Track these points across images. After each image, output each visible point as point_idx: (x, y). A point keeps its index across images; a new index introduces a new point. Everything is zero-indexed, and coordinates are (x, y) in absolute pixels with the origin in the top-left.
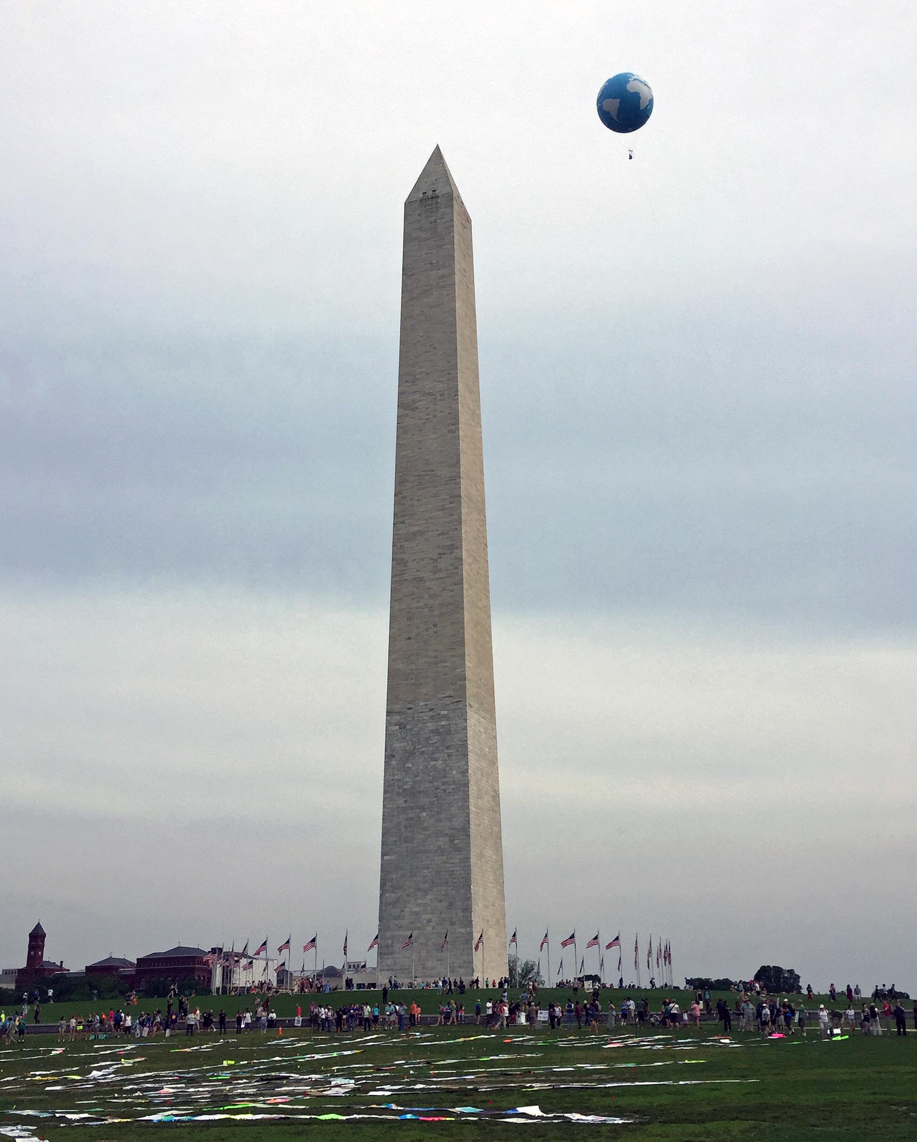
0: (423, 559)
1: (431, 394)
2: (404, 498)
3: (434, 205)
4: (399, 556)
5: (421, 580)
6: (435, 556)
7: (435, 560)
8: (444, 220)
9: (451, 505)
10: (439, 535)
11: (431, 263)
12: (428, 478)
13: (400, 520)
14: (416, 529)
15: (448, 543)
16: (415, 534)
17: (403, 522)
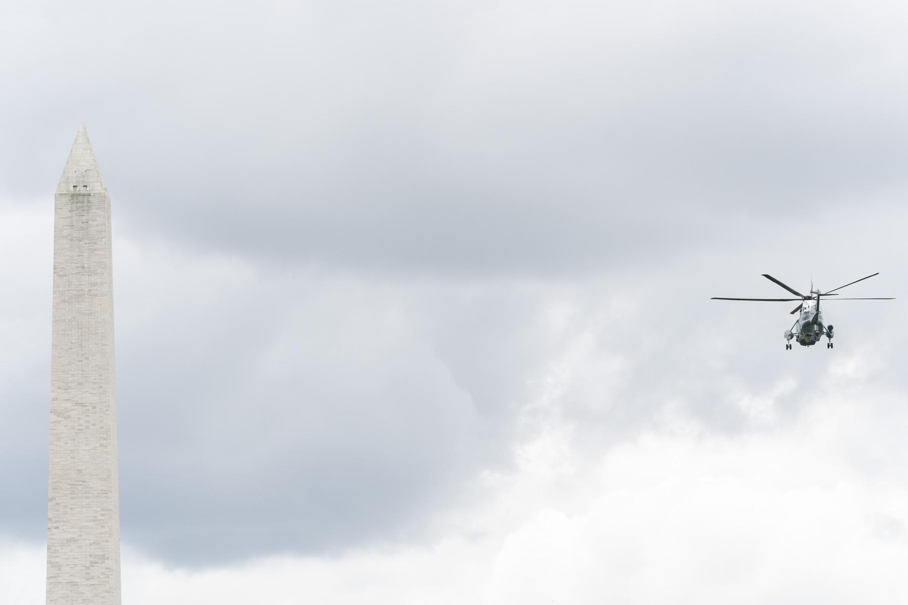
0: (76, 565)
1: (82, 405)
2: (58, 504)
3: (86, 204)
4: (53, 560)
5: (75, 584)
6: (88, 564)
7: (88, 568)
8: (95, 223)
9: (103, 518)
10: (91, 544)
11: (83, 267)
12: (80, 488)
13: (55, 525)
14: (69, 536)
15: (100, 553)
16: (69, 541)
17: (57, 528)
